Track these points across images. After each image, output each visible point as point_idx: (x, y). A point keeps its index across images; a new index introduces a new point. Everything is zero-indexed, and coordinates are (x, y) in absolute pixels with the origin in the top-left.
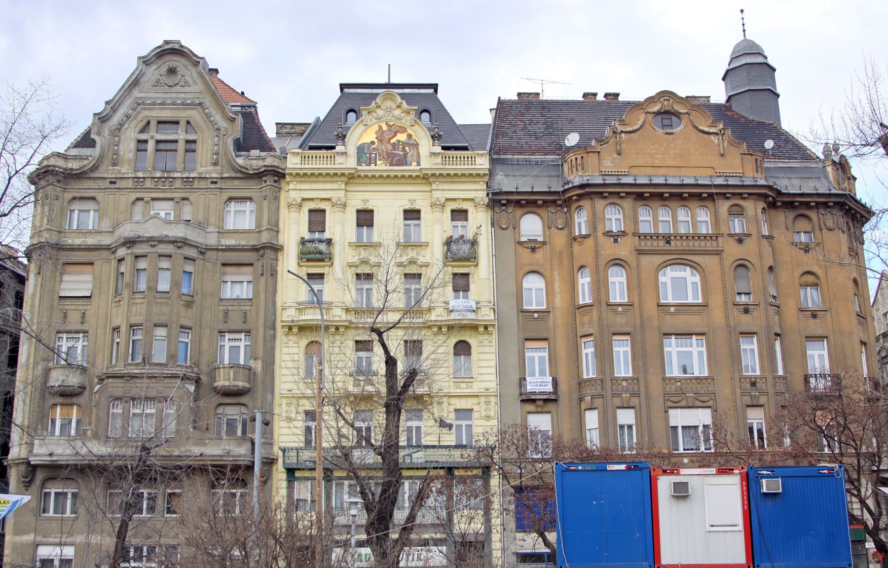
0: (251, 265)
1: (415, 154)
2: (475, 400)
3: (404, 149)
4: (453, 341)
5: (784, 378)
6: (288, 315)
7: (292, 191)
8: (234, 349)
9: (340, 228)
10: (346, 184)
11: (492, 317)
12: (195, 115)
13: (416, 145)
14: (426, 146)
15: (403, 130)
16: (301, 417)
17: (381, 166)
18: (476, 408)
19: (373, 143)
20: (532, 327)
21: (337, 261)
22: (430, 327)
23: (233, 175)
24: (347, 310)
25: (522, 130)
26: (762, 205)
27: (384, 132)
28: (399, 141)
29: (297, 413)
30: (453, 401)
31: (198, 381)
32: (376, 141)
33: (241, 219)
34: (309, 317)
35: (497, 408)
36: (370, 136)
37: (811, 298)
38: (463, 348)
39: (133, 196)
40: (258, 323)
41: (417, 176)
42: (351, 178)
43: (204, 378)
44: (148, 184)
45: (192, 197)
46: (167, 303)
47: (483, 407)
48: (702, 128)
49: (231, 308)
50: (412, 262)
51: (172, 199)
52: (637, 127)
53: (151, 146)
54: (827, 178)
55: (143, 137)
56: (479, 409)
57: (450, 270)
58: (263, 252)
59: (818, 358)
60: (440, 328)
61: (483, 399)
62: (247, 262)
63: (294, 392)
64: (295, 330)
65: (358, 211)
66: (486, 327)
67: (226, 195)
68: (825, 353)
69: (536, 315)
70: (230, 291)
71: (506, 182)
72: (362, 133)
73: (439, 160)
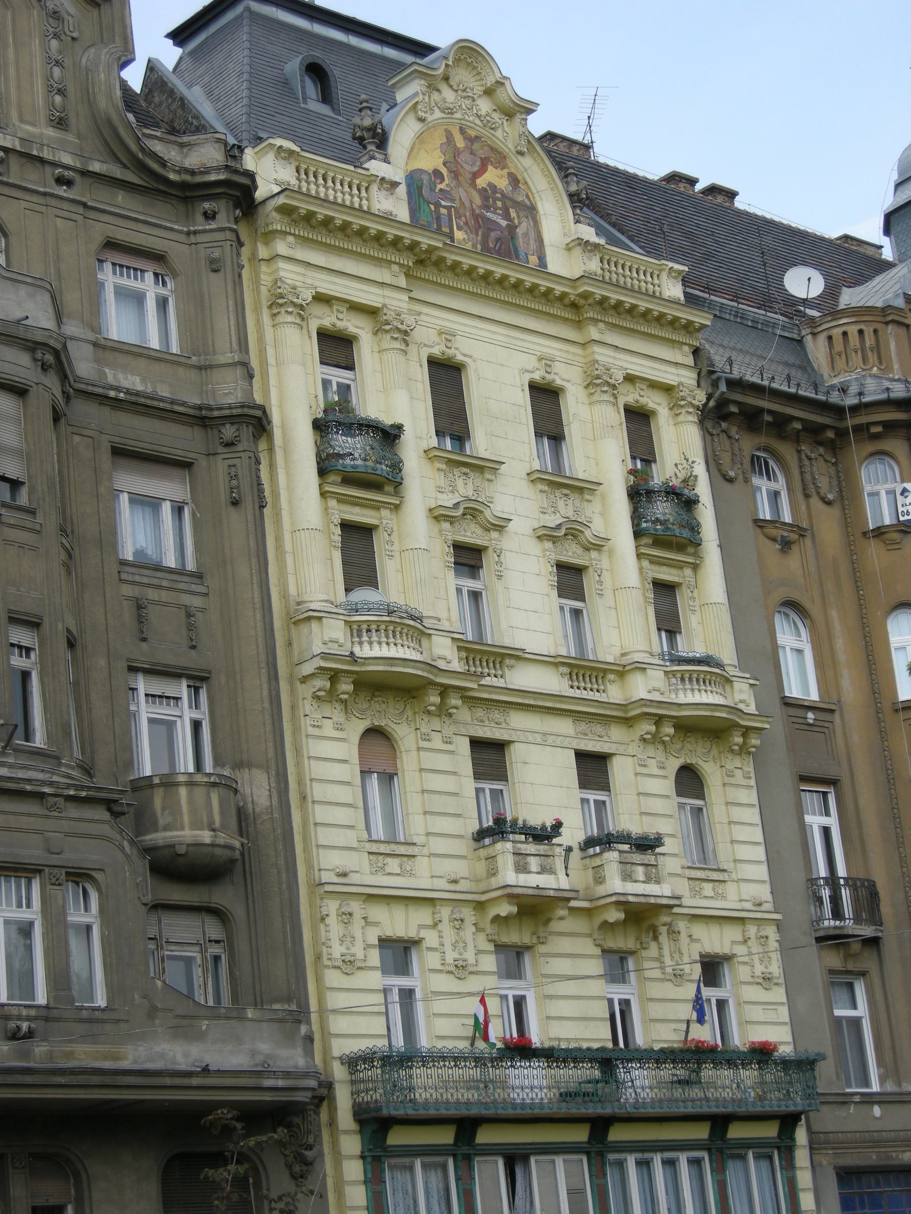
0: (186, 465)
1: (532, 235)
3: (507, 216)
7: (295, 266)
13: (531, 210)
19: (437, 173)
23: (117, 172)
27: (457, 152)
32: (444, 171)
46: (34, 548)
49: (152, 594)
62: (178, 454)
63: (354, 878)
67: (101, 229)
69: (810, 715)
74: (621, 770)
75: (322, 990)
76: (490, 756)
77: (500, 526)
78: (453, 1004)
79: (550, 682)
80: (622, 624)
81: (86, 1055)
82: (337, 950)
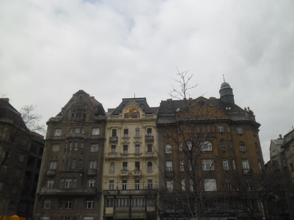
2: (153, 177)
4: (147, 162)
5: (236, 170)
6: (106, 156)
7: (109, 125)
8: (93, 165)
9: (120, 134)
10: (122, 123)
11: (157, 155)
12: (86, 107)
14: (141, 113)
15: (136, 109)
16: (109, 182)
17: (130, 118)
18: (153, 179)
19: (128, 113)
20: (168, 158)
21: (119, 142)
22: (141, 158)
24: (121, 154)
25: (166, 108)
26: (227, 124)
28: (135, 112)
29: (108, 181)
30: (147, 177)
31: (83, 173)
33: (96, 132)
34: (111, 156)
35: (159, 179)
36: (128, 111)
37: (243, 148)
38: (150, 164)
39: (70, 127)
40: (100, 158)
41: (139, 121)
42: (123, 122)
43: (85, 172)
44: (74, 124)
45: (84, 127)
47: (155, 179)
48: (210, 105)
50: (137, 142)
51: (79, 128)
52: (194, 106)
53: (75, 115)
54: (246, 116)
55: (74, 113)
56: (154, 180)
57: (147, 144)
58: (101, 140)
59: (246, 165)
60: (144, 158)
61: (155, 177)
64: (108, 160)
65: (124, 130)
66: (156, 158)
68: (248, 163)
70: (92, 150)
71: (161, 121)
72: (126, 111)
73: (144, 116)
74: (141, 163)
75: (102, 185)
76: (125, 164)
77: (129, 143)
78: (118, 185)
79: (133, 156)
80: (143, 149)
81: (73, 191)
82: (104, 182)
